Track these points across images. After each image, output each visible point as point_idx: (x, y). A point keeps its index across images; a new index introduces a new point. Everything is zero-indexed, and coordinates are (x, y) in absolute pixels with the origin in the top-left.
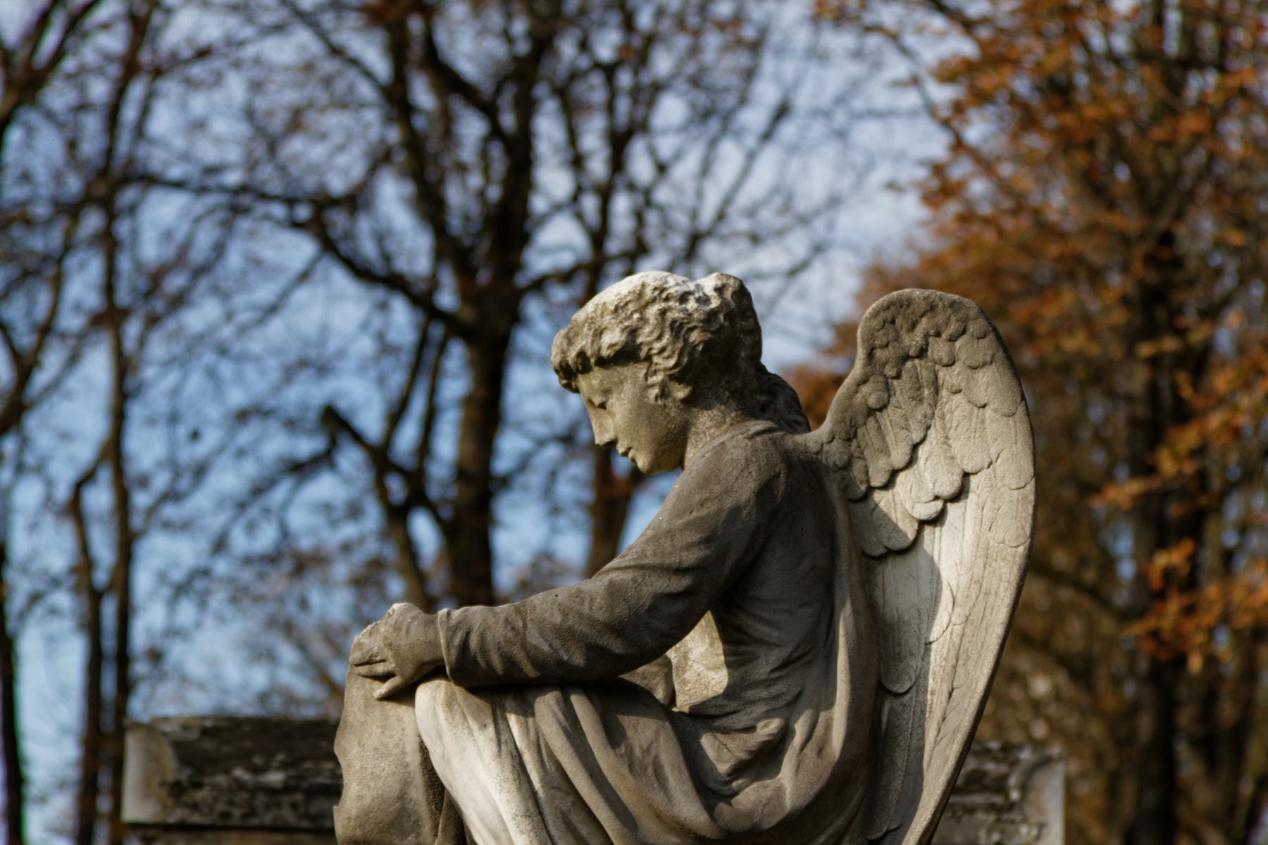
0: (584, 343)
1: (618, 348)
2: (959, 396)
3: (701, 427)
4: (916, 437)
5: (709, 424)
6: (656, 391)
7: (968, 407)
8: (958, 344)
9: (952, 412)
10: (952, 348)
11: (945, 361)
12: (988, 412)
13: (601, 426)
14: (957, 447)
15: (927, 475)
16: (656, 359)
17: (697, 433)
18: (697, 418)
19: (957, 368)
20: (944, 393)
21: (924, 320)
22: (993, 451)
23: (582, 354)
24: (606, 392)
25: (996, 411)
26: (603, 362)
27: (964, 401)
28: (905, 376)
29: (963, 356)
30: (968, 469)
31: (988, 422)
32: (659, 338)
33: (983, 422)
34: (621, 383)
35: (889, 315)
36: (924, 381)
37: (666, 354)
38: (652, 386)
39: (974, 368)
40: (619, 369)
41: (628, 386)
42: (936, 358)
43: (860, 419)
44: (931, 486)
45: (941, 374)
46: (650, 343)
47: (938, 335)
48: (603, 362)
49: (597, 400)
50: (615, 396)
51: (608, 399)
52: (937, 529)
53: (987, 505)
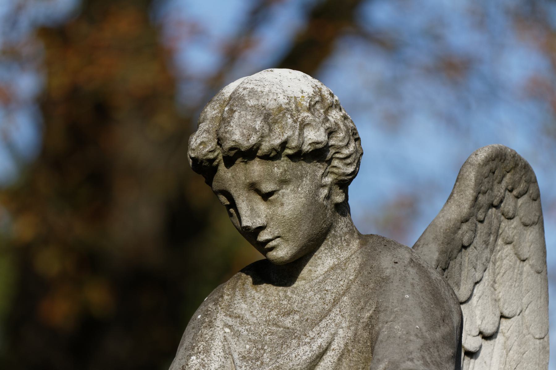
0: (288, 133)
1: (320, 146)
2: (510, 247)
3: (339, 232)
4: (478, 276)
5: (345, 230)
6: (325, 192)
7: (514, 258)
8: (520, 201)
9: (502, 260)
10: (516, 203)
11: (510, 215)
12: (526, 267)
13: (252, 210)
14: (501, 292)
15: (478, 312)
16: (335, 163)
17: (335, 236)
18: (337, 222)
19: (515, 222)
20: (500, 241)
21: (508, 176)
22: (525, 300)
23: (284, 145)
24: (284, 182)
25: (532, 266)
26: (299, 156)
27: (512, 252)
28: (486, 222)
29: (521, 213)
30: (506, 313)
31: (524, 275)
32: (347, 145)
33: (521, 274)
34: (302, 177)
35: (492, 165)
36: (493, 231)
37: (349, 161)
38: (323, 186)
39: (526, 225)
40: (304, 164)
41: (306, 181)
42: (506, 210)
43: (455, 252)
44: (479, 322)
45: (503, 224)
46: (341, 147)
47: (511, 191)
48: (299, 156)
49: (267, 187)
50: (291, 187)
51: (282, 188)
52: (472, 360)
53: (515, 348)
